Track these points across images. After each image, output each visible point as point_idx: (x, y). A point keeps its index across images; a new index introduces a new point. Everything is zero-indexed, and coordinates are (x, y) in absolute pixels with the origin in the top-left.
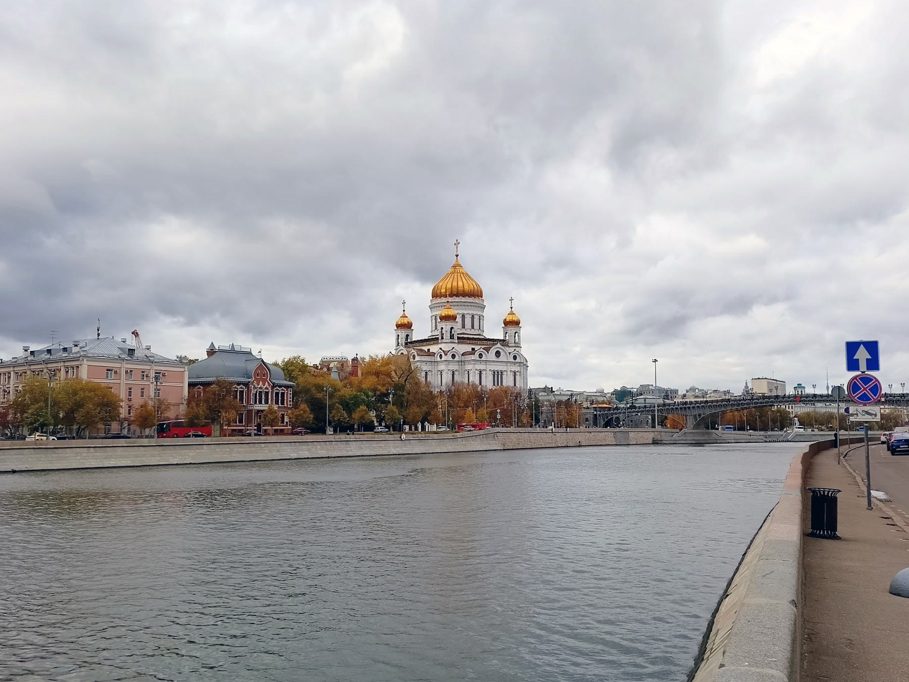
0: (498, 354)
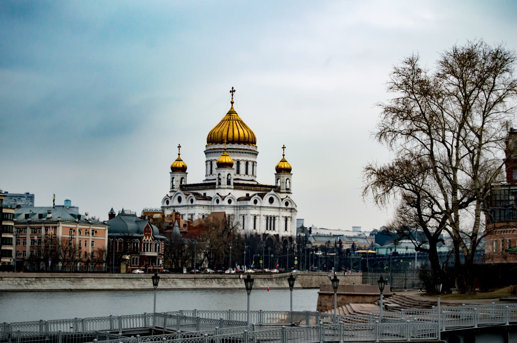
0: (271, 200)
